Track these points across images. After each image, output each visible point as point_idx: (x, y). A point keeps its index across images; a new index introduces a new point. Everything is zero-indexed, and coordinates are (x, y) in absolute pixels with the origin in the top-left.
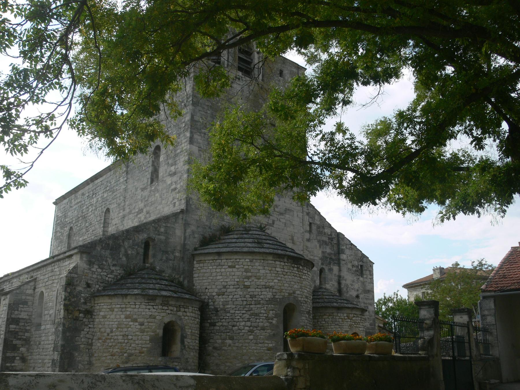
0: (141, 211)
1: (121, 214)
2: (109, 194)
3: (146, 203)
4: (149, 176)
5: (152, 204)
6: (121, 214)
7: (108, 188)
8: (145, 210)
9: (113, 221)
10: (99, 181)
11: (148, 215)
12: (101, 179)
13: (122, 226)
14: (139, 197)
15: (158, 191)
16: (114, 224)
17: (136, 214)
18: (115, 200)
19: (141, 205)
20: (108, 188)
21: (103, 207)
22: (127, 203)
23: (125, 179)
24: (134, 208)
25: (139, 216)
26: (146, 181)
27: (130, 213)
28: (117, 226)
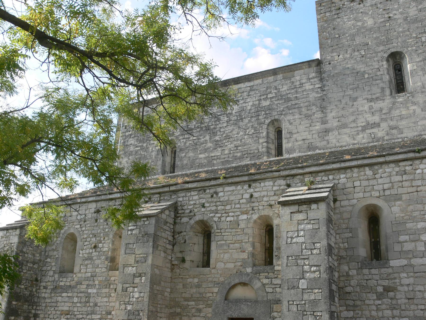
0: (377, 125)
1: (317, 128)
2: (276, 102)
3: (384, 116)
4: (386, 86)
5: (401, 117)
6: (317, 128)
7: (270, 96)
8: (384, 125)
9: (295, 136)
10: (242, 85)
11: (394, 131)
12: (248, 84)
13: (325, 143)
14: (366, 108)
15: (414, 103)
16: (300, 138)
17: (360, 129)
18: (296, 110)
19: (376, 118)
20: (270, 96)
21: (260, 117)
22: (330, 116)
23: (317, 86)
24: (354, 121)
25: (368, 131)
26: (376, 90)
27: (344, 126)
28: (307, 142)
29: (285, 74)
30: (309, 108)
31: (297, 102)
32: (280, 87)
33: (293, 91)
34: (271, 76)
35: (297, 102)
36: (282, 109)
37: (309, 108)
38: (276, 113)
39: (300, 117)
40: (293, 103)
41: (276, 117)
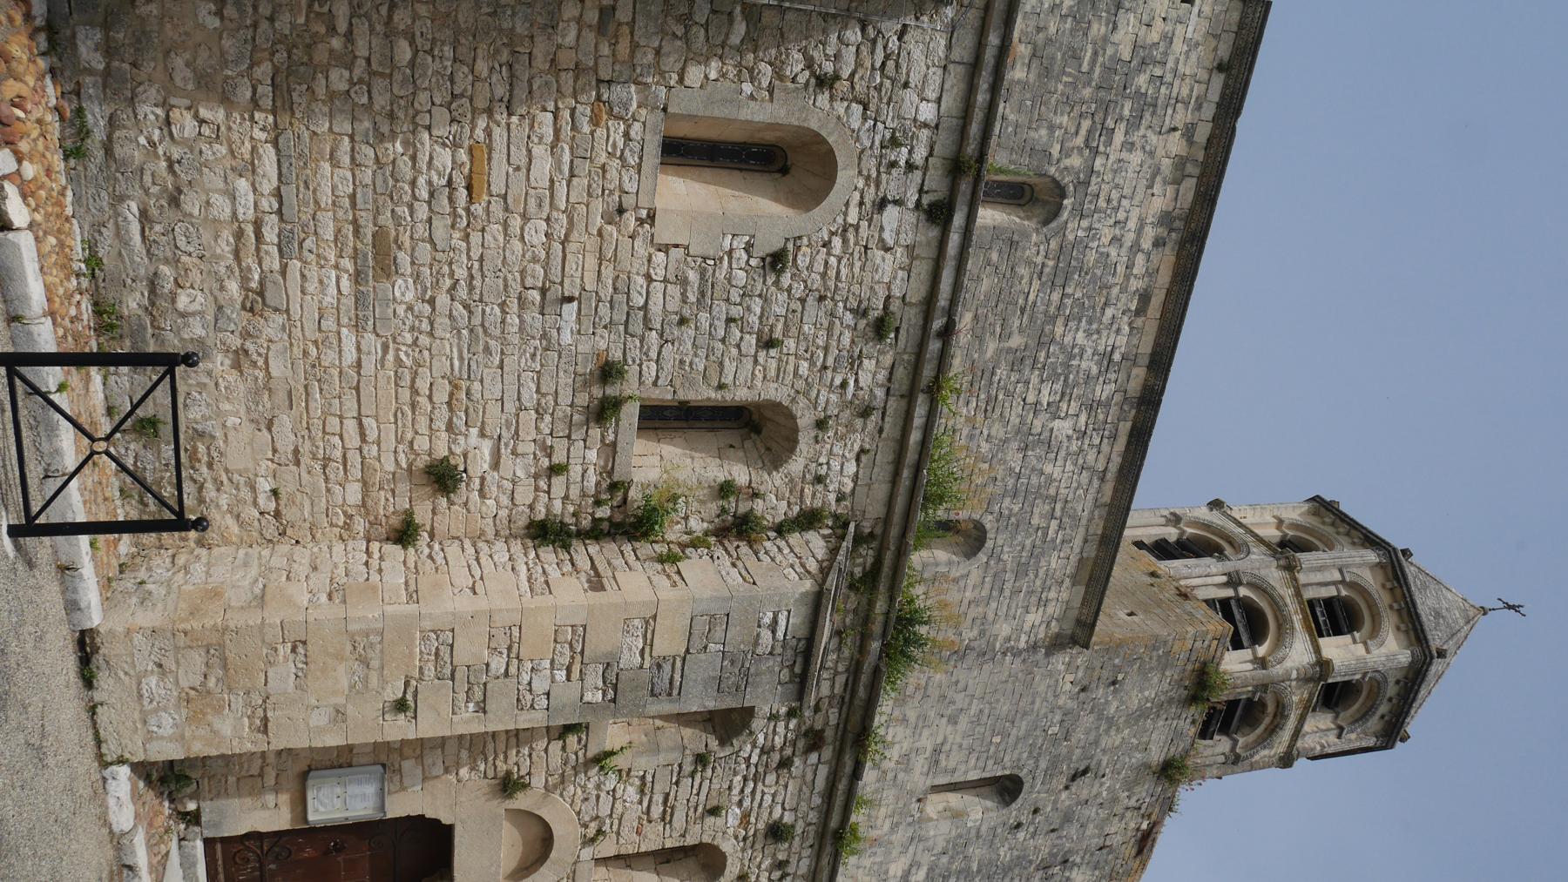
2: (1028, 542)
29: (1090, 563)
30: (978, 622)
31: (1007, 593)
32: (1066, 550)
33: (1038, 582)
34: (1105, 528)
35: (1007, 593)
36: (1005, 557)
37: (978, 622)
38: (1000, 542)
39: (966, 602)
40: (1008, 586)
41: (989, 544)
